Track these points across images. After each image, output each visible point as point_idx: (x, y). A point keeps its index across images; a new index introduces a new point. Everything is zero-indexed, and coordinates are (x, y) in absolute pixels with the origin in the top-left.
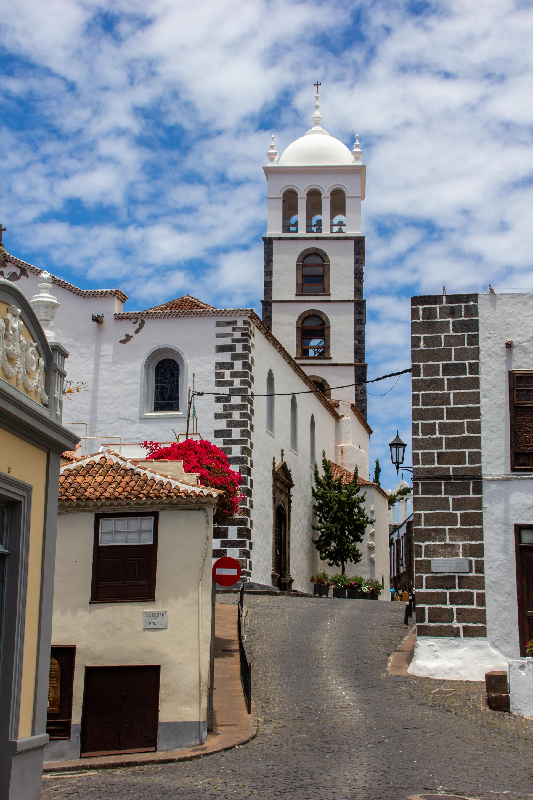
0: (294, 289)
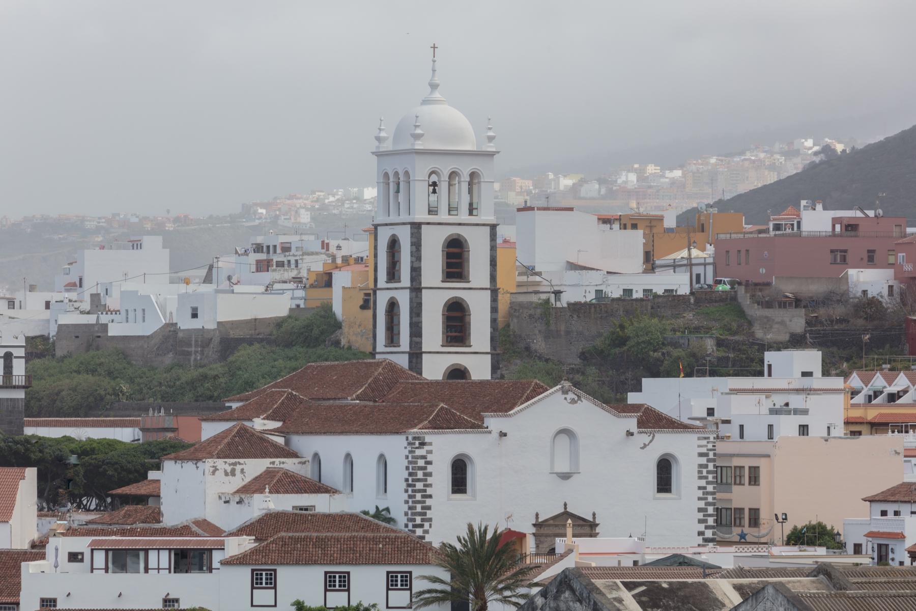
0: (440, 276)
